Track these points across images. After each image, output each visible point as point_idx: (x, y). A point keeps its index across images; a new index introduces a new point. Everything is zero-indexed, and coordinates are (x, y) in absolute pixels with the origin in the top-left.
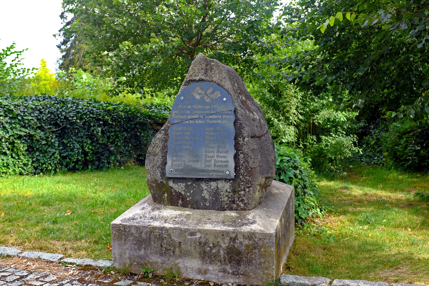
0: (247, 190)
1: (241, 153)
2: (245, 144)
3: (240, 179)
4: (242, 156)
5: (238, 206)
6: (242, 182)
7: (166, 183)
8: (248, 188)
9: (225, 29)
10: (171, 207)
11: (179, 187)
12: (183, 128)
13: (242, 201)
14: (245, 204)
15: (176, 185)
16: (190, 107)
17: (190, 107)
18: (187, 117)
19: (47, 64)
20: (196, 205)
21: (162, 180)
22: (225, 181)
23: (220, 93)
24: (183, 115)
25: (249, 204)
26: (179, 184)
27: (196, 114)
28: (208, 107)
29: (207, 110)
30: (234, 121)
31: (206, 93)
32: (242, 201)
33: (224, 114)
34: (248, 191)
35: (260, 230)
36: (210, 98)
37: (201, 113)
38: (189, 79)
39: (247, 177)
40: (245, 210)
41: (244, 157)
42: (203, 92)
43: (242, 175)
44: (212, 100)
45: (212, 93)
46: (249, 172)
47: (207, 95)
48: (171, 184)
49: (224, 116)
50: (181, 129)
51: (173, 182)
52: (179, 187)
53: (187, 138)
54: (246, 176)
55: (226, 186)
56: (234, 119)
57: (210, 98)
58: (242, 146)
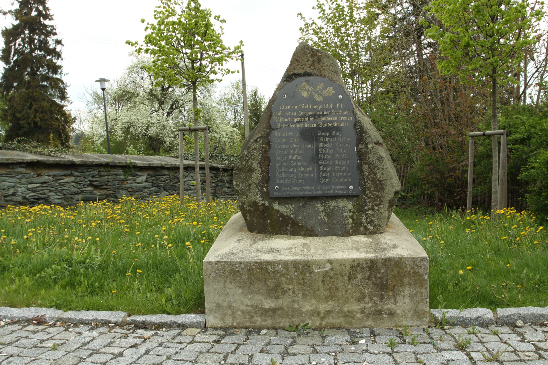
0: (376, 208)
1: (365, 163)
2: (368, 152)
3: (367, 195)
4: (366, 166)
5: (366, 228)
6: (369, 198)
7: (270, 205)
8: (377, 205)
9: (502, 19)
10: (276, 236)
11: (284, 209)
12: (288, 134)
13: (371, 222)
14: (375, 226)
15: (283, 207)
16: (296, 107)
17: (296, 107)
18: (293, 120)
19: (244, 53)
20: (310, 233)
21: (263, 202)
22: (347, 199)
23: (334, 90)
24: (287, 117)
25: (380, 226)
26: (287, 206)
27: (305, 115)
28: (319, 107)
29: (318, 111)
30: (353, 123)
31: (315, 89)
32: (371, 222)
33: (341, 116)
34: (378, 210)
35: (409, 254)
36: (321, 95)
37: (311, 115)
38: (291, 73)
39: (375, 193)
40: (375, 233)
41: (369, 168)
42: (311, 89)
43: (369, 190)
44: (324, 97)
45: (324, 89)
46: (377, 186)
47: (317, 92)
48: (276, 206)
49: (341, 118)
50: (286, 135)
51: (279, 204)
52: (284, 209)
53: (295, 146)
54: (374, 191)
55: (348, 205)
56: (354, 120)
57: (321, 95)
58: (366, 154)
